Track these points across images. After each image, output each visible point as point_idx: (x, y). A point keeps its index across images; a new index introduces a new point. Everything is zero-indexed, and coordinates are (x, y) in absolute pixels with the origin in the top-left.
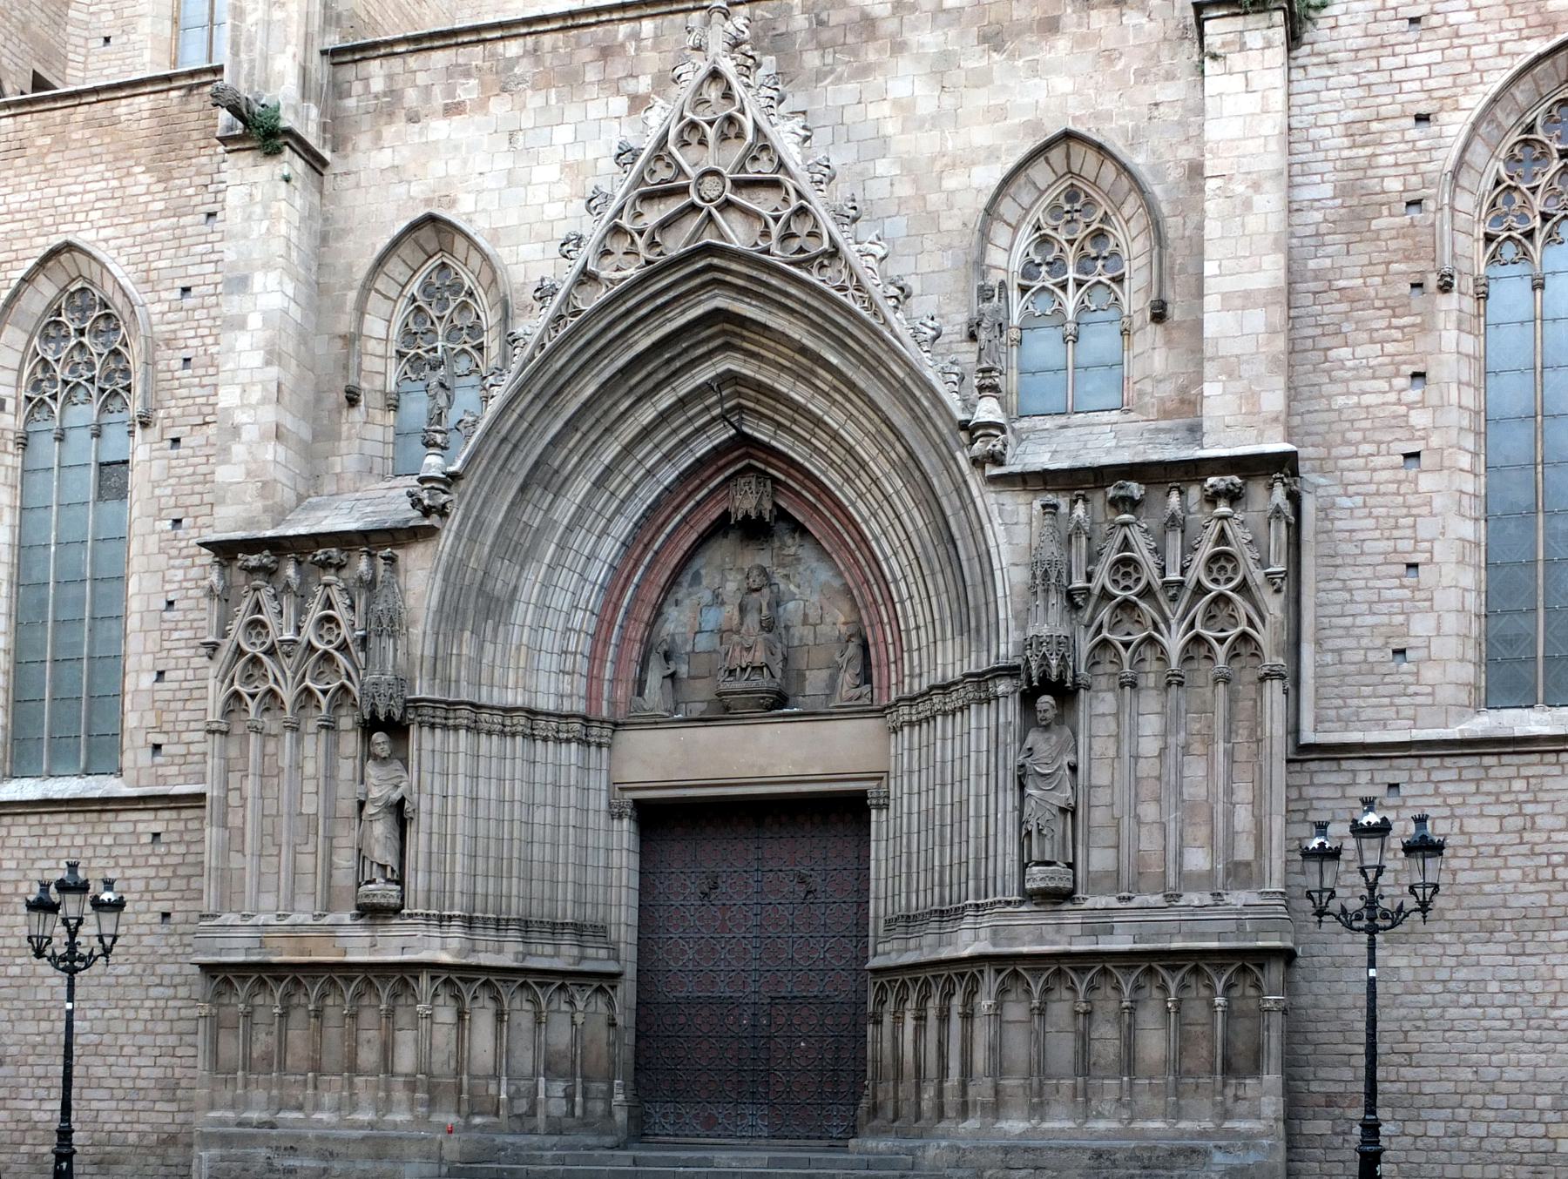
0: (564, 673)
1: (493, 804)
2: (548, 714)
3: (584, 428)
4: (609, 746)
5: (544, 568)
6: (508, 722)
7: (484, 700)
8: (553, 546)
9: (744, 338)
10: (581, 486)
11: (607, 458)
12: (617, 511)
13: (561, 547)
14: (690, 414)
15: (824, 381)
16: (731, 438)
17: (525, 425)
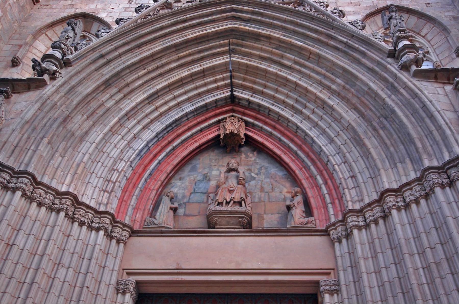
0: (105, 191)
1: (25, 253)
2: (88, 207)
3: (150, 68)
4: (125, 244)
5: (108, 128)
6: (57, 202)
7: (46, 180)
8: (116, 119)
9: (242, 46)
10: (141, 96)
11: (159, 87)
12: (157, 119)
13: (120, 123)
14: (207, 80)
15: (289, 59)
16: (226, 98)
17: (117, 53)
